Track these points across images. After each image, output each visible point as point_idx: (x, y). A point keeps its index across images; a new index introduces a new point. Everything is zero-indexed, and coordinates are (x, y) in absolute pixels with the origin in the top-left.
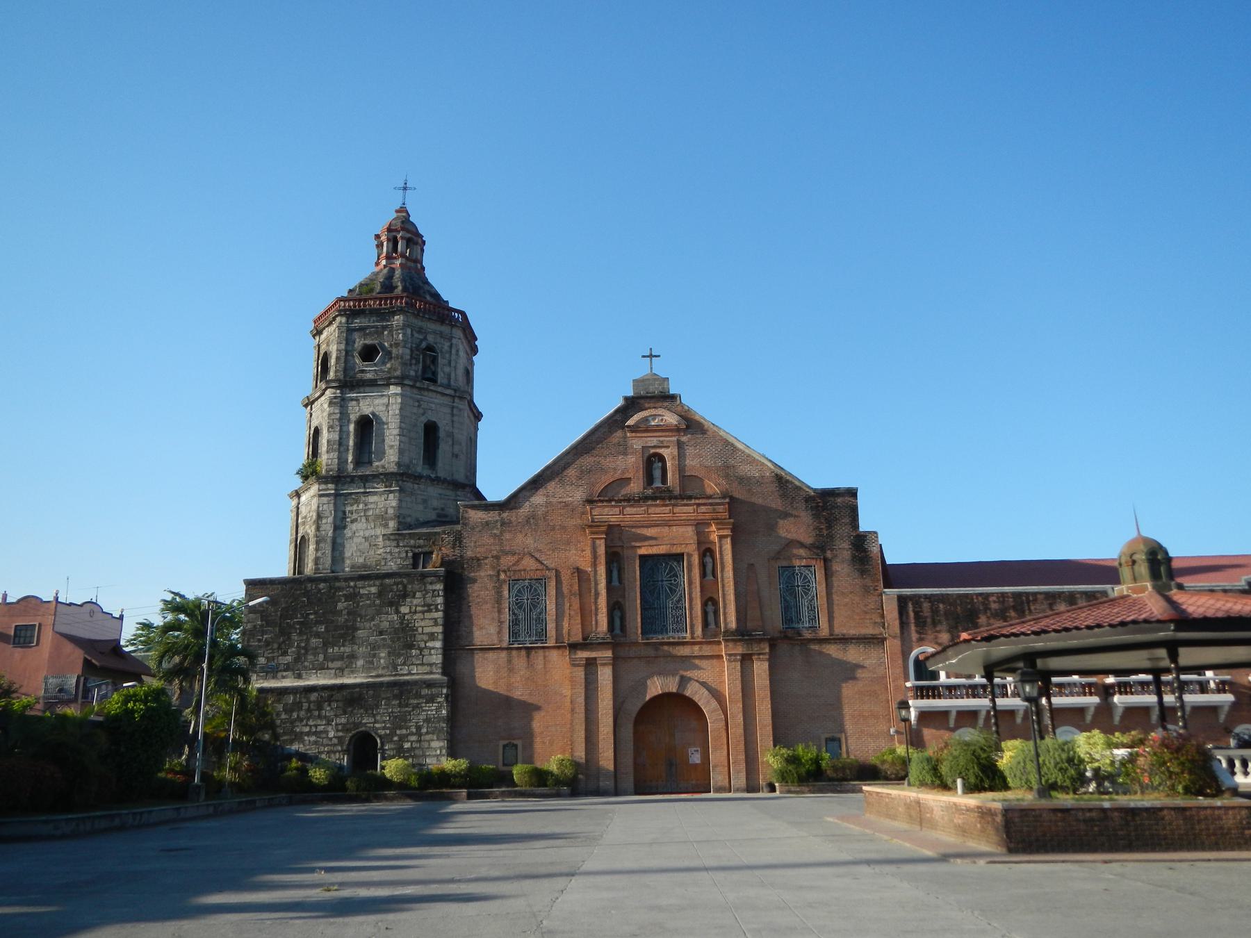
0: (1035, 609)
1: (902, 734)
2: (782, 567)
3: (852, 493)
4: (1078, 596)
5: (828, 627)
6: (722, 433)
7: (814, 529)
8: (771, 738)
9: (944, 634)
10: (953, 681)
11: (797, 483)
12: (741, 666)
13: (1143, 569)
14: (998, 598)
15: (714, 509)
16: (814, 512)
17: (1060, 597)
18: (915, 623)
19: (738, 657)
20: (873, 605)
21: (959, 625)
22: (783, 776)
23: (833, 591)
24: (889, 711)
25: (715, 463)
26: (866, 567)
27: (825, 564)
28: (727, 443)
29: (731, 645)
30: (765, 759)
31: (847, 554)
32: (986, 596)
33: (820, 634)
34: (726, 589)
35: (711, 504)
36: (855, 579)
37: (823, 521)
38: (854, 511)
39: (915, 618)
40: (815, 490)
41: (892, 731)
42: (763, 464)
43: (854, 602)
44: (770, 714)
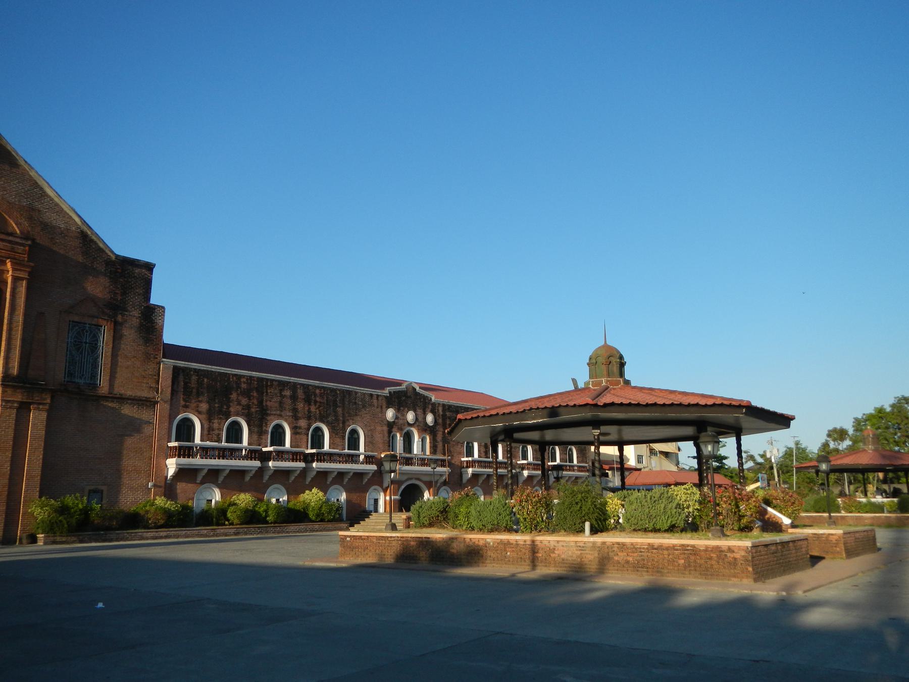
0: (271, 392)
1: (160, 487)
2: (73, 321)
3: (150, 267)
4: (298, 386)
5: (108, 386)
6: (32, 174)
7: (110, 292)
8: (38, 489)
9: (204, 404)
10: (208, 443)
11: (101, 245)
12: (16, 415)
13: (615, 369)
14: (247, 379)
15: (13, 248)
16: (112, 276)
17: (287, 385)
18: (183, 392)
19: (16, 405)
20: (151, 371)
21: (216, 398)
22: (51, 528)
23: (120, 353)
24: (150, 467)
25: (19, 201)
26: (151, 336)
27: (114, 327)
28: (36, 185)
29: (9, 391)
30: (30, 510)
31: (135, 322)
32: (239, 377)
33: (100, 391)
34: (14, 333)
35: (10, 242)
36: (139, 345)
37: (119, 286)
38: (148, 284)
39: (184, 388)
40: (117, 256)
41: (150, 484)
42: (70, 217)
43: (135, 366)
44: (41, 464)
